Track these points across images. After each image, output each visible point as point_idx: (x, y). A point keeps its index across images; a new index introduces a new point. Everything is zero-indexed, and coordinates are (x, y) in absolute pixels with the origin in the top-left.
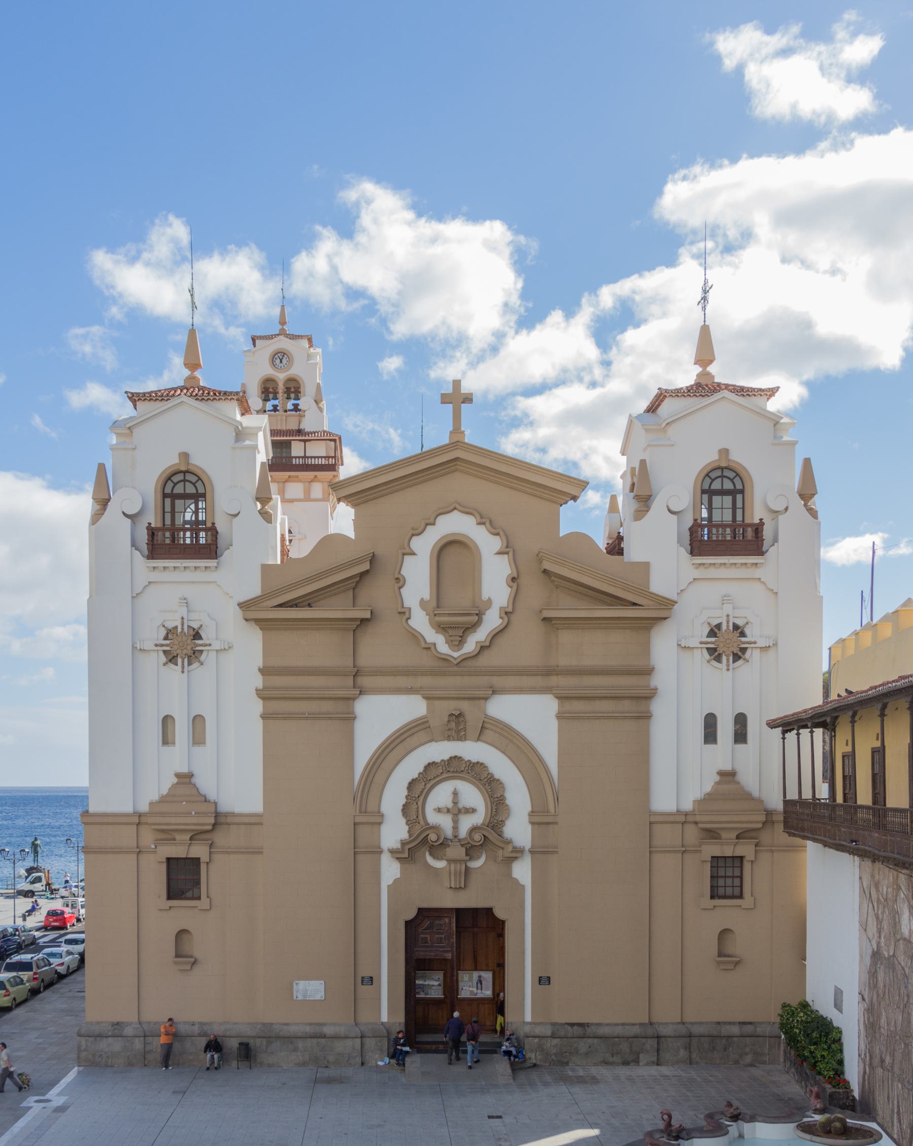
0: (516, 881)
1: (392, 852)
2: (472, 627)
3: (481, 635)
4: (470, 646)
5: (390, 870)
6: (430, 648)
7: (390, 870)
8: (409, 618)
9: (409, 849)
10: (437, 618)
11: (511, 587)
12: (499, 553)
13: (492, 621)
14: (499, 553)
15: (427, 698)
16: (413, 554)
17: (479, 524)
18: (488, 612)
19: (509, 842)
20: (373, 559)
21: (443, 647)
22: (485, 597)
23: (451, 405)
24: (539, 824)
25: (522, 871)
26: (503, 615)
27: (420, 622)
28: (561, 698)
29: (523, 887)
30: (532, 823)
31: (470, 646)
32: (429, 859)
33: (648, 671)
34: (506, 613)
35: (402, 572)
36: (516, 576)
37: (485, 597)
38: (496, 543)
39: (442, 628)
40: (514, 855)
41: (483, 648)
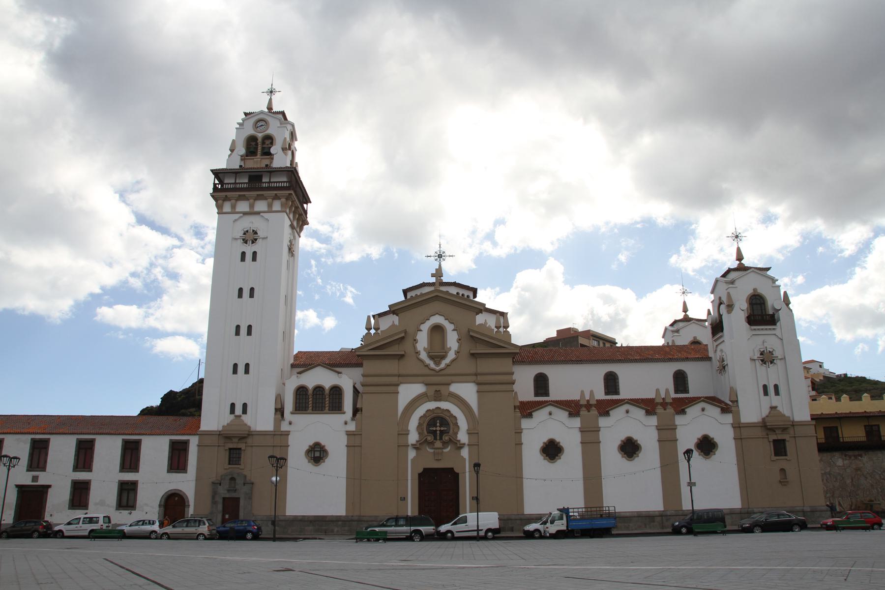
0: (462, 457)
1: (412, 445)
2: (443, 357)
3: (447, 361)
4: (442, 365)
5: (412, 454)
6: (427, 366)
7: (412, 454)
8: (420, 355)
9: (420, 444)
10: (430, 354)
11: (458, 342)
12: (453, 330)
13: (451, 356)
14: (453, 330)
15: (426, 384)
16: (421, 330)
17: (446, 319)
18: (450, 352)
19: (459, 441)
20: (405, 332)
21: (432, 365)
22: (448, 347)
23: (435, 278)
24: (471, 433)
25: (465, 453)
26: (456, 353)
27: (423, 356)
28: (478, 384)
29: (465, 459)
30: (468, 433)
31: (442, 365)
32: (429, 450)
33: (512, 374)
34: (458, 352)
35: (417, 337)
36: (460, 338)
37: (448, 347)
38: (452, 327)
39: (431, 358)
40: (462, 446)
41: (448, 365)
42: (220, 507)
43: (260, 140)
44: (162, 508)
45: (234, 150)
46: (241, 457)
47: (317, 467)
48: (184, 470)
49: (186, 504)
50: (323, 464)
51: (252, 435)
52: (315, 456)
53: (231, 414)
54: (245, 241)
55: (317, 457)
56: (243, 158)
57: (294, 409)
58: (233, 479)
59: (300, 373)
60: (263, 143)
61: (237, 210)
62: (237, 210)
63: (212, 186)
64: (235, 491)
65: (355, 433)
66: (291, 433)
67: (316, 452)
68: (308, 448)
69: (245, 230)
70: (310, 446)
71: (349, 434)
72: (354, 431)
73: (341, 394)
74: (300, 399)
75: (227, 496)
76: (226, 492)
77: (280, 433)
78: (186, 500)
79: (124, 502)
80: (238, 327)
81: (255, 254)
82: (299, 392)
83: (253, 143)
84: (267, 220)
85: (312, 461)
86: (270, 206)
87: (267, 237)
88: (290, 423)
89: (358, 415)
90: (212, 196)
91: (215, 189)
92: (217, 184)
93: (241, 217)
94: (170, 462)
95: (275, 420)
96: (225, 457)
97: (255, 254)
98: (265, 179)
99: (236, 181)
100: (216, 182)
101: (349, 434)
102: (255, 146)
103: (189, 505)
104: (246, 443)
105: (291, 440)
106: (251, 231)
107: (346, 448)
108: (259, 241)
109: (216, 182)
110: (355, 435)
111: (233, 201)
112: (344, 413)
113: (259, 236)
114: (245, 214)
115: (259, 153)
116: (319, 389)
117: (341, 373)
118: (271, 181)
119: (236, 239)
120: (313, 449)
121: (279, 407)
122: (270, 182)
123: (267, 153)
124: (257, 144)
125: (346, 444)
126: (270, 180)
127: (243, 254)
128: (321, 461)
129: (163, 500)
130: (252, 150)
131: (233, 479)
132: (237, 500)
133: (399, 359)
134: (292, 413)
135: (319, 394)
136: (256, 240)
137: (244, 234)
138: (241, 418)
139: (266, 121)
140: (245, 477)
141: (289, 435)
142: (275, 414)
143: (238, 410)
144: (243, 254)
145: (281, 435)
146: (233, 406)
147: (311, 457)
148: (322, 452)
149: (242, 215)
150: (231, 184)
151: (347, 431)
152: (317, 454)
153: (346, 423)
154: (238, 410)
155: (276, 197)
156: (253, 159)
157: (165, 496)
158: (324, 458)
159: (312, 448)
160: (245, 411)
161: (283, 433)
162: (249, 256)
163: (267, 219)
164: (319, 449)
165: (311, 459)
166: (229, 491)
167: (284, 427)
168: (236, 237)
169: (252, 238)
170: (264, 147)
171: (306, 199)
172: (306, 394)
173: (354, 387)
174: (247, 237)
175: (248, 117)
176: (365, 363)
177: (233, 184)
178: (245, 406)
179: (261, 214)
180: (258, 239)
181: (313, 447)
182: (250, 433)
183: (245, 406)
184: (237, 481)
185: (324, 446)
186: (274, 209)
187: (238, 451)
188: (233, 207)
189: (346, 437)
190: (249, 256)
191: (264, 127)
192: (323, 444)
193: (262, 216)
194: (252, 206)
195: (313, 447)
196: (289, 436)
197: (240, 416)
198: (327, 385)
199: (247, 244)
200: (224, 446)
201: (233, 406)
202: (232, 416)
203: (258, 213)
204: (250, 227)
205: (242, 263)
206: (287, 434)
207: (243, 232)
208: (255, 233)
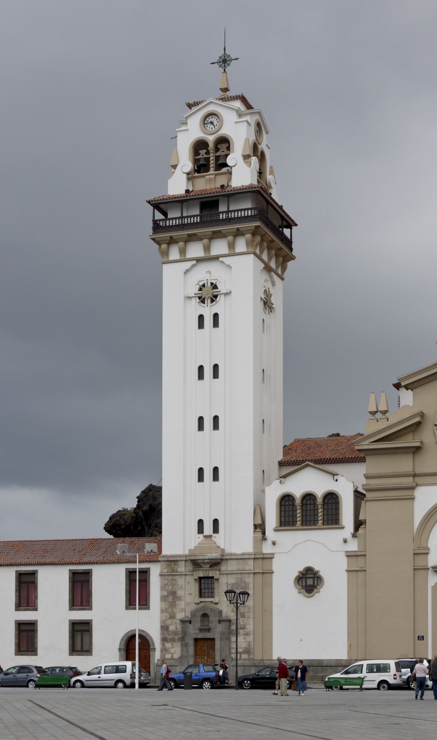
42: (191, 650)
43: (211, 145)
44: (123, 653)
45: (176, 165)
46: (214, 588)
47: (310, 599)
48: (146, 605)
49: (151, 647)
50: (317, 594)
51: (227, 560)
52: (308, 584)
53: (199, 533)
54: (202, 300)
55: (310, 586)
56: (190, 177)
57: (278, 524)
58: (205, 616)
59: (285, 477)
60: (217, 149)
62: (189, 255)
63: (151, 225)
64: (209, 630)
65: (357, 554)
66: (275, 555)
67: (308, 580)
68: (296, 574)
69: (201, 284)
70: (300, 572)
71: (350, 555)
72: (355, 551)
73: (339, 503)
74: (285, 511)
75: (200, 636)
76: (198, 631)
77: (261, 556)
78: (150, 643)
79: (78, 646)
80: (201, 420)
82: (283, 503)
83: (203, 152)
84: (229, 267)
85: (304, 590)
86: (231, 246)
87: (231, 292)
88: (274, 543)
89: (361, 531)
90: (153, 239)
91: (157, 227)
92: (160, 220)
94: (128, 595)
95: (255, 539)
96: (194, 588)
98: (222, 208)
99: (182, 214)
100: (156, 219)
101: (350, 555)
102: (206, 156)
103: (155, 649)
104: (219, 570)
105: (276, 565)
106: (209, 285)
107: (346, 573)
108: (221, 299)
109: (156, 219)
110: (357, 556)
111: (181, 244)
112: (343, 528)
113: (220, 291)
114: (199, 260)
115: (211, 166)
116: (309, 497)
117: (337, 475)
118: (230, 209)
119: (190, 298)
120: (304, 576)
121: (259, 522)
122: (228, 212)
123: (221, 165)
124: (208, 153)
125: (345, 567)
126: (228, 208)
127: (201, 318)
128: (315, 590)
129: (123, 643)
130: (202, 165)
131: (205, 616)
132: (213, 639)
133: (414, 453)
134: (276, 530)
135: (310, 504)
136: (216, 297)
137: (200, 289)
138: (213, 539)
139: (219, 115)
140: (220, 612)
141: (272, 558)
142: (254, 532)
143: (208, 529)
144: (201, 318)
145: (263, 558)
146: (201, 522)
147: (303, 586)
148: (316, 579)
149: (194, 262)
150: (176, 218)
151: (346, 552)
152: (310, 582)
153: (345, 541)
154: (208, 529)
155: (238, 233)
156: (204, 176)
157: (126, 638)
158: (318, 587)
159: (303, 574)
160: (216, 530)
161: (265, 556)
162: (208, 321)
163: (229, 266)
164: (312, 576)
165: (302, 589)
166: (201, 630)
167: (267, 548)
168: (190, 296)
169: (211, 295)
170: (219, 156)
171: (287, 221)
172: (293, 505)
173: (356, 492)
174: (204, 294)
175: (194, 109)
176: (368, 459)
177: (179, 218)
178: (216, 522)
179: (221, 259)
181: (304, 573)
182: (224, 557)
183: (216, 522)
184: (210, 618)
185: (317, 572)
187: (210, 580)
188: (183, 252)
189: (345, 560)
190: (208, 321)
191: (213, 126)
192: (316, 568)
193: (222, 262)
194: (207, 249)
195: (304, 573)
196: (274, 560)
197: (210, 536)
198: (320, 492)
199: (204, 303)
200: (193, 575)
201: (201, 522)
202: (201, 536)
203: (216, 258)
204: (207, 280)
205: (201, 330)
206: (270, 558)
207: (198, 287)
208: (214, 286)
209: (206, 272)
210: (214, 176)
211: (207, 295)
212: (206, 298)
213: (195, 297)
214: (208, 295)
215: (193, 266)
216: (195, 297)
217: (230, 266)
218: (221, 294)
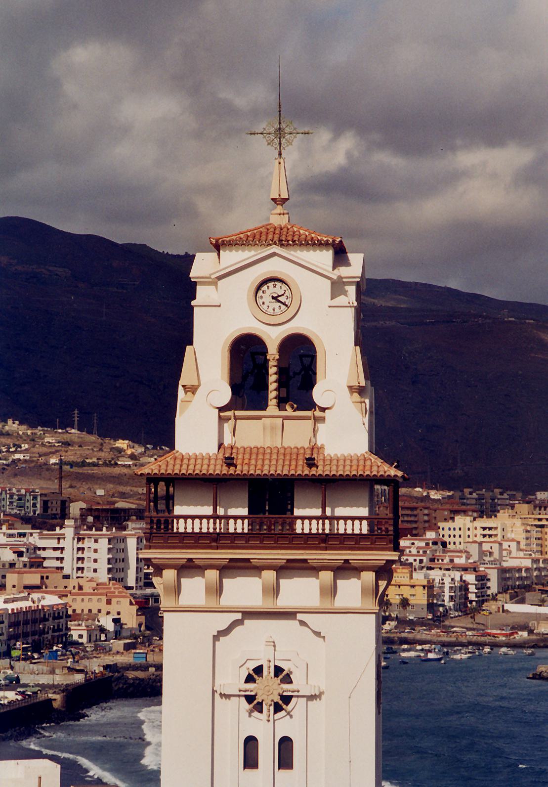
61: (226, 600)
81: (285, 744)
87: (321, 693)
93: (236, 623)
97: (285, 744)
127: (251, 743)
144: (251, 743)
155: (345, 570)
156: (259, 418)
162: (267, 753)
180: (294, 700)
186: (340, 601)
190: (267, 753)
193: (302, 623)
199: (261, 712)
209: (267, 642)
210: (282, 419)
211: (268, 695)
212: (264, 702)
213: (239, 696)
214: (271, 698)
215: (236, 623)
216: (239, 696)
217: (322, 635)
218: (298, 696)
